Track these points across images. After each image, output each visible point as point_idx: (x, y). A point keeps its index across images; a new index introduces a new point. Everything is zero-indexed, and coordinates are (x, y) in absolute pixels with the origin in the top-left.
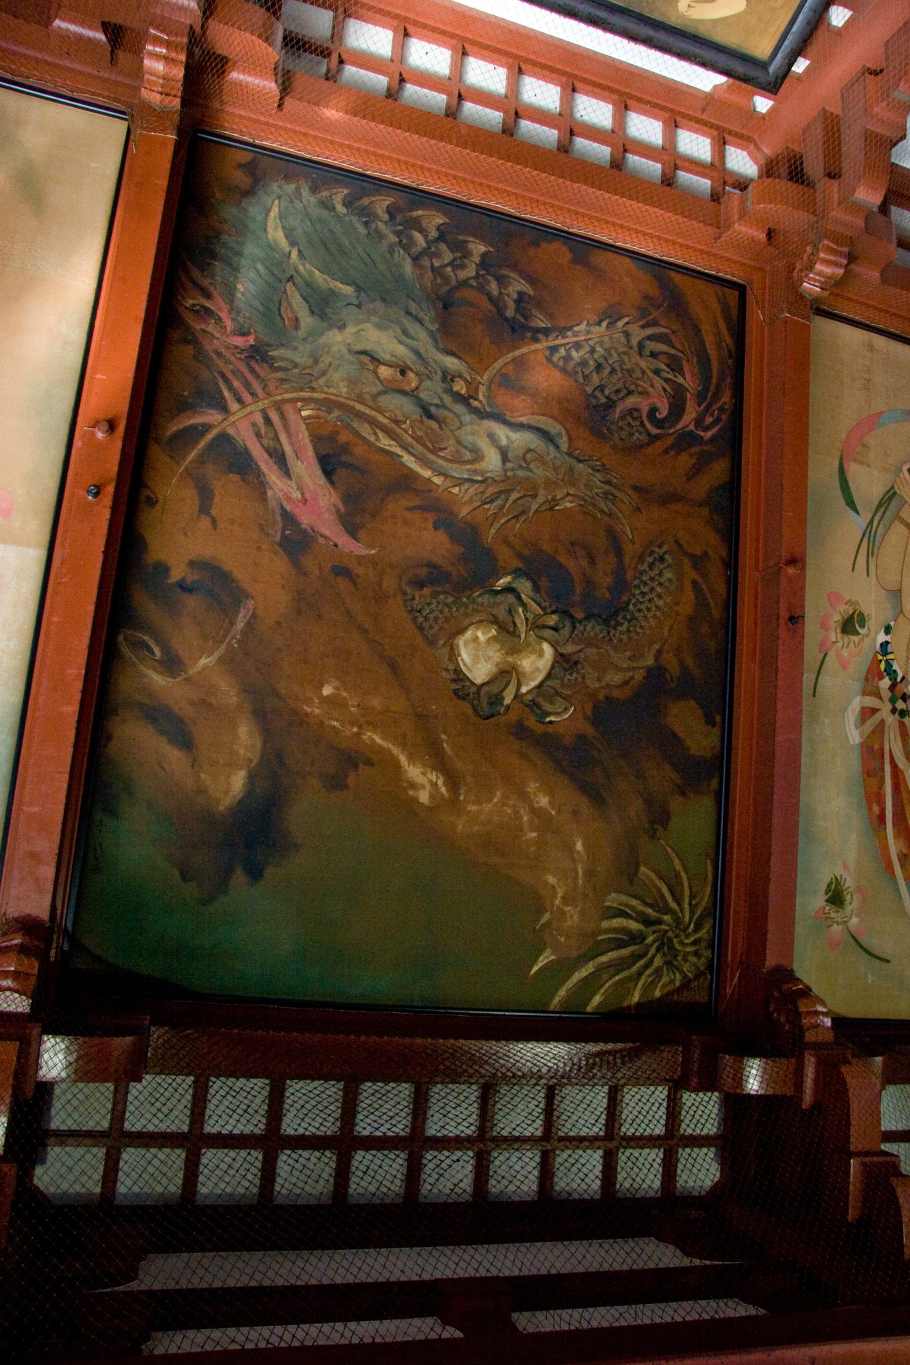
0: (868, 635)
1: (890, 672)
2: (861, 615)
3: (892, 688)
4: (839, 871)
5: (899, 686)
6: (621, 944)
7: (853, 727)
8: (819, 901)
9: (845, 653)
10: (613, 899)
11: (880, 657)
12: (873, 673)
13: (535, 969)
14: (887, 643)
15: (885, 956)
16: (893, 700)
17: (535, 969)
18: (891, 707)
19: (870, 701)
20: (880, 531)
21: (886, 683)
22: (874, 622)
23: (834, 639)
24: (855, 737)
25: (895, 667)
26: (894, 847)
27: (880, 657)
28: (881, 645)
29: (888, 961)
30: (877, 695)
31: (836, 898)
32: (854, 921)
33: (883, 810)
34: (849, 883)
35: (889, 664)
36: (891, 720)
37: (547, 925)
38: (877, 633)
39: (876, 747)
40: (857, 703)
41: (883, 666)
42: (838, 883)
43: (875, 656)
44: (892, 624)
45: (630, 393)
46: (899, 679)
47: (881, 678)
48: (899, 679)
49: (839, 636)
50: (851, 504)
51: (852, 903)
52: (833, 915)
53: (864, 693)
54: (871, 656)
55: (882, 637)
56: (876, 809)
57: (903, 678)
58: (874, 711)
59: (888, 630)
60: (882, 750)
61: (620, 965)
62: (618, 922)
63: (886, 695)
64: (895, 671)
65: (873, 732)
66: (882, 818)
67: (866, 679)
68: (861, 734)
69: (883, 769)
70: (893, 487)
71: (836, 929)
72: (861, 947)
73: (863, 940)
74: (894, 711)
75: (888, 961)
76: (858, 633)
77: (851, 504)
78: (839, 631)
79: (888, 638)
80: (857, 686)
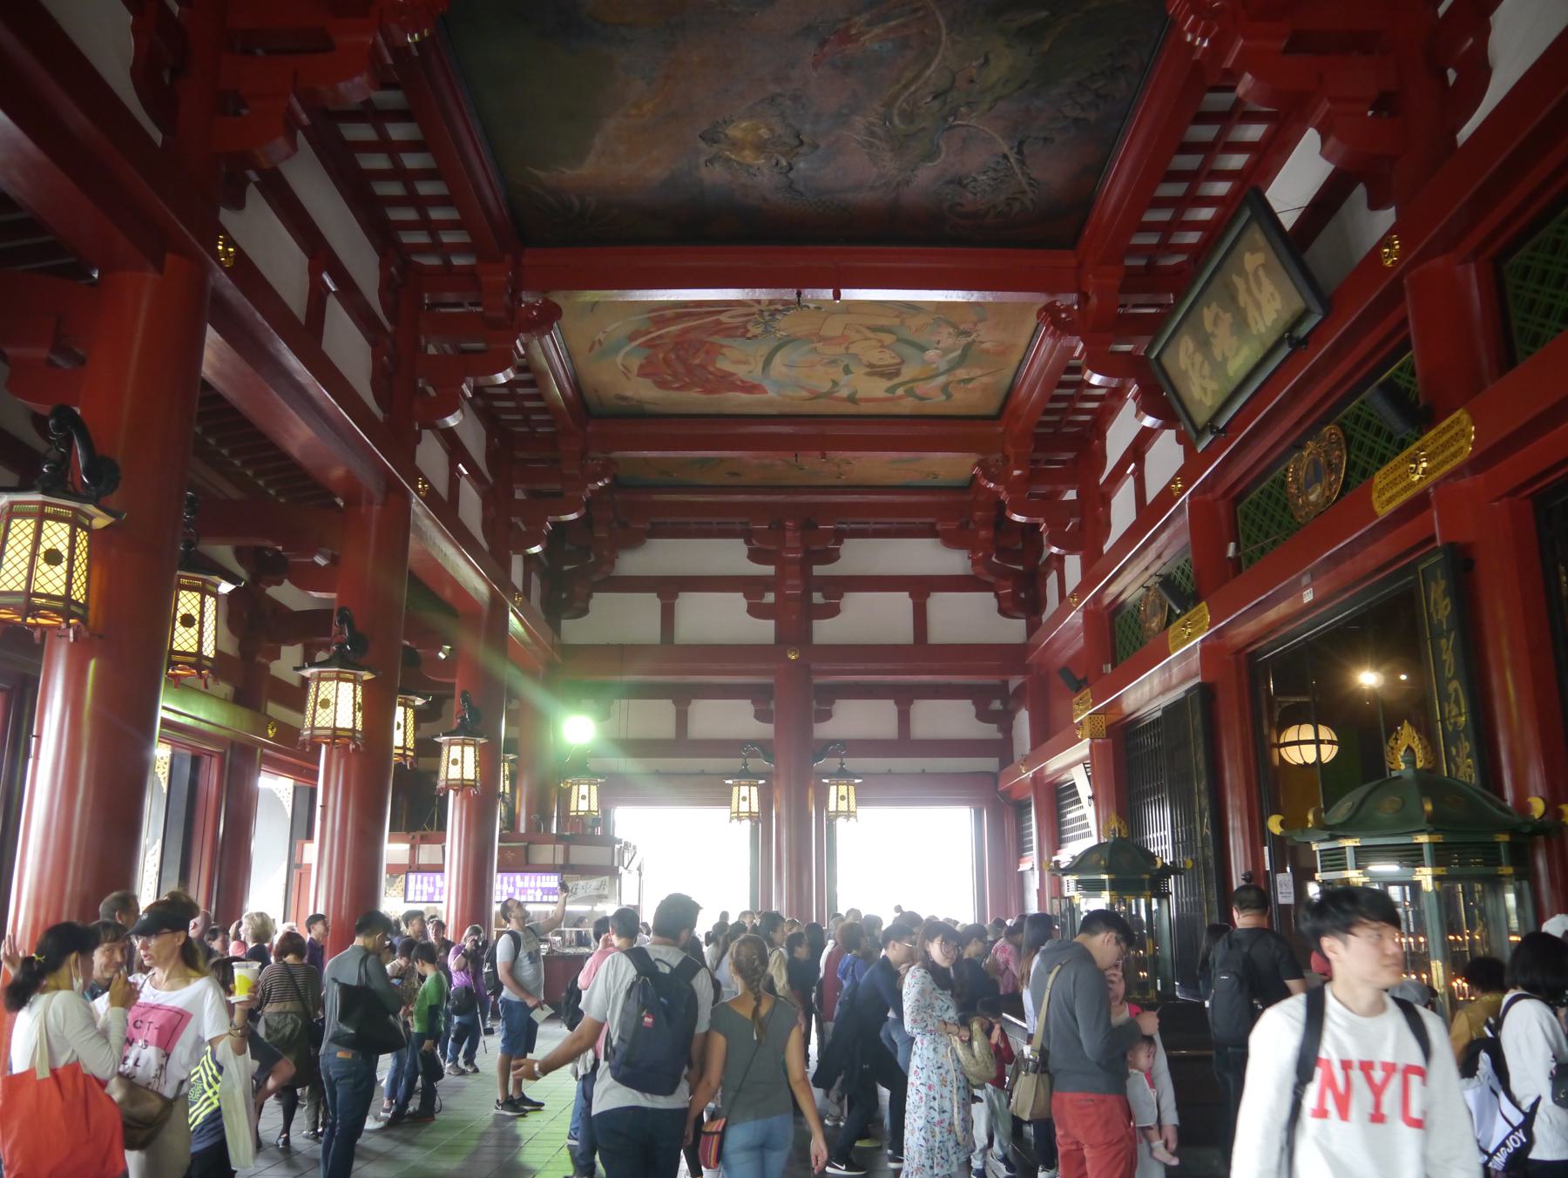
21: (780, 307)
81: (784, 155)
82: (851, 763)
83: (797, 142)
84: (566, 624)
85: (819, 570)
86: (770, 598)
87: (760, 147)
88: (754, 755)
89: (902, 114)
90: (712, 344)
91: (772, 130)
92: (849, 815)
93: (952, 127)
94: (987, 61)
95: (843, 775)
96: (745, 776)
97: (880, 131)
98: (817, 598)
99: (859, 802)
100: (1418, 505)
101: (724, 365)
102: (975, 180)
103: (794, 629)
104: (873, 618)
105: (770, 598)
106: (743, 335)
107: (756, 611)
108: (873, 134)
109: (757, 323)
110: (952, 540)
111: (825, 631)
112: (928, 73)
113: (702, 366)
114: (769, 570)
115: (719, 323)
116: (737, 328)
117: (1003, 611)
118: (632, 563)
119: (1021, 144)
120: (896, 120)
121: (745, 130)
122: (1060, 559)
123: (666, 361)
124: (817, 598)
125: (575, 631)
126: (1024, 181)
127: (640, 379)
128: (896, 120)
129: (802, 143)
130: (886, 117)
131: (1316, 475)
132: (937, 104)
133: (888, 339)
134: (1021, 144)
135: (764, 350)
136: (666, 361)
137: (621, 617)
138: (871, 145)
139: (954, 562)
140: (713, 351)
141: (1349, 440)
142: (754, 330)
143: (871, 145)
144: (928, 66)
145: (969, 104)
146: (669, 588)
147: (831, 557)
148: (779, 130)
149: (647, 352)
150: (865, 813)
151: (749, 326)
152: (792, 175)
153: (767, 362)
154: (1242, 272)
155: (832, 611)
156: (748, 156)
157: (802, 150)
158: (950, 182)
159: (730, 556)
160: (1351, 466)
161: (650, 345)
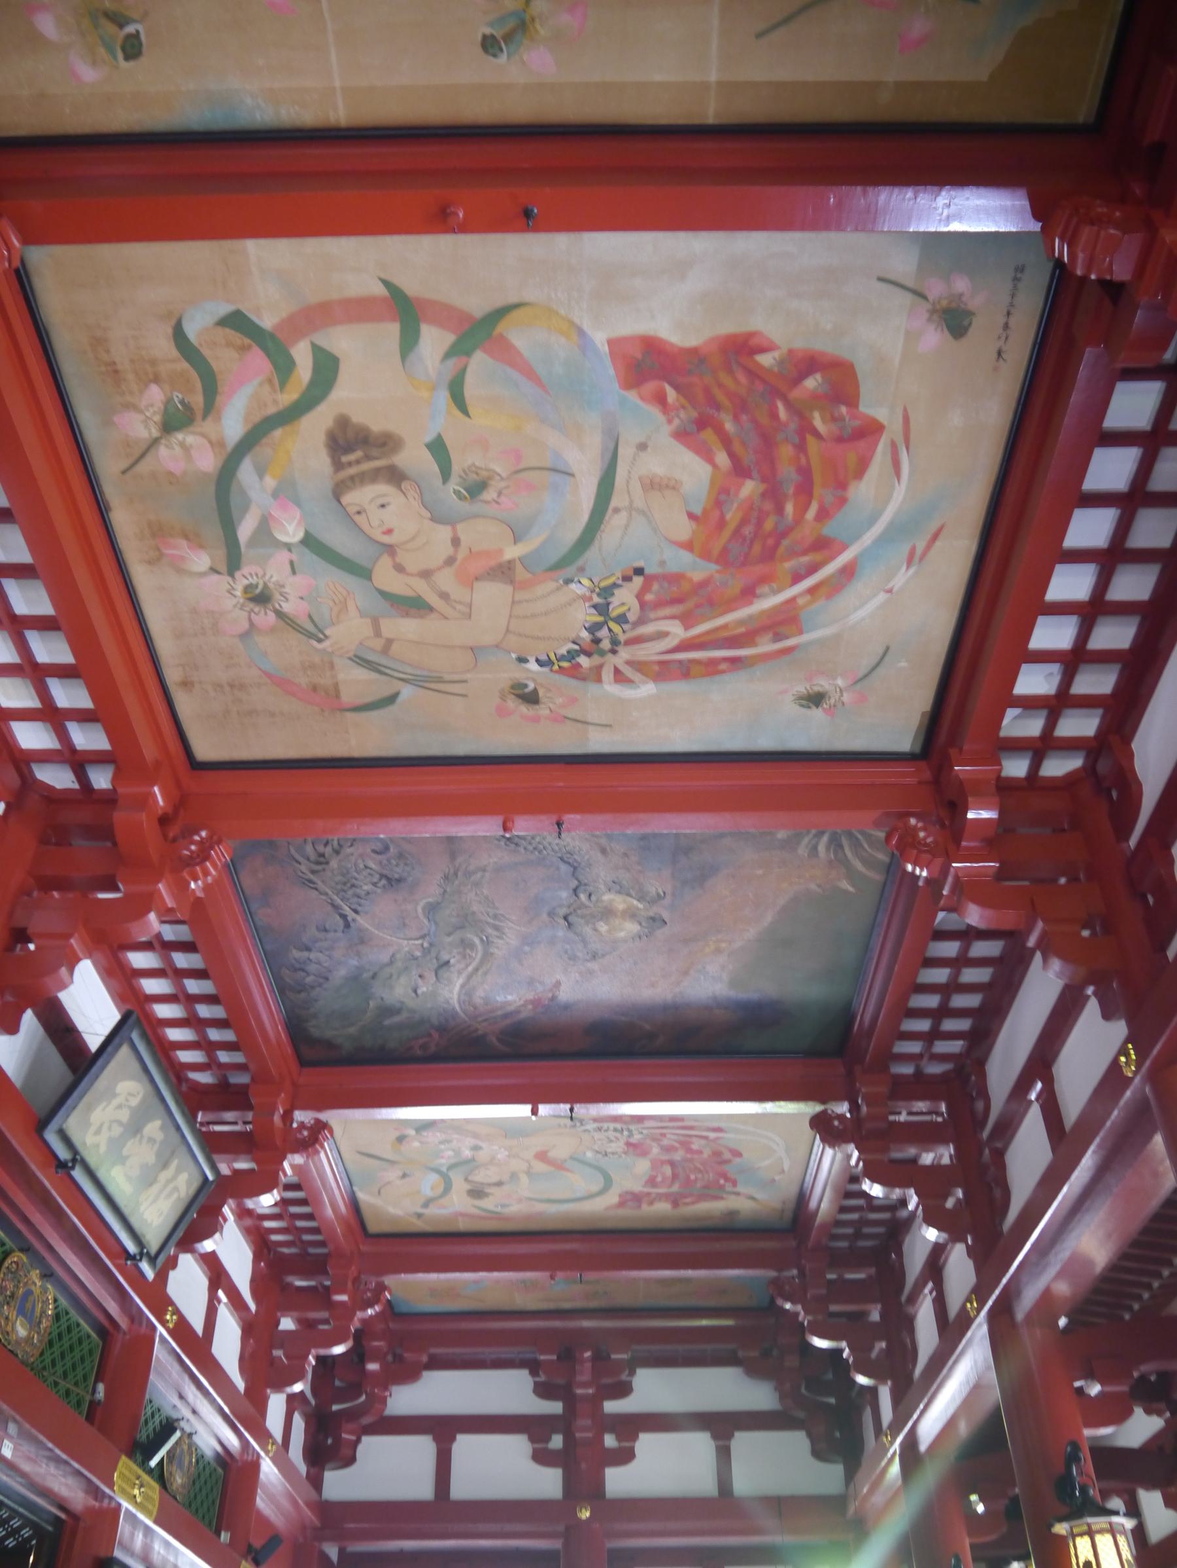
0: (534, 680)
1: (571, 656)
2: (513, 687)
3: (589, 654)
4: (789, 698)
5: (587, 648)
6: (841, 846)
7: (639, 691)
8: (817, 713)
9: (560, 701)
10: (802, 850)
11: (556, 667)
12: (574, 671)
13: (851, 889)
14: (537, 660)
15: (881, 651)
16: (602, 653)
17: (851, 889)
18: (610, 655)
19: (607, 675)
20: (409, 670)
21: (583, 660)
22: (516, 673)
23: (548, 712)
24: (648, 689)
25: (563, 651)
26: (766, 646)
27: (556, 667)
28: (541, 666)
29: (888, 648)
30: (599, 668)
31: (815, 699)
32: (840, 682)
33: (726, 659)
34: (802, 688)
35: (561, 658)
36: (624, 654)
37: (819, 886)
38: (528, 670)
39: (656, 668)
40: (610, 687)
41: (565, 664)
42: (801, 698)
43: (556, 672)
44: (514, 656)
45: (366, 867)
46: (577, 647)
47: (579, 665)
48: (577, 647)
49: (542, 706)
50: (392, 699)
51: (822, 684)
52: (832, 701)
53: (599, 680)
54: (557, 677)
55: (533, 666)
56: (723, 666)
57: (574, 642)
58: (617, 671)
59: (522, 660)
60: (662, 663)
61: (856, 845)
62: (822, 848)
63: (596, 660)
64: (568, 652)
65: (640, 671)
66: (734, 661)
67: (584, 679)
68: (645, 683)
69: (680, 662)
70: (350, 659)
71: (846, 697)
72: (866, 676)
73: (860, 675)
74: (614, 652)
75: (888, 648)
76: (535, 691)
77: (392, 699)
78: (537, 707)
79: (532, 660)
80: (592, 688)
81: (583, 906)
83: (570, 919)
87: (608, 913)
89: (472, 946)
90: (705, 555)
91: (596, 930)
93: (423, 937)
94: (415, 992)
97: (490, 931)
98: (610, 1441)
102: (375, 884)
106: (649, 580)
108: (497, 928)
109: (622, 619)
112: (460, 981)
113: (740, 471)
115: (687, 620)
116: (659, 604)
119: (347, 925)
120: (477, 941)
121: (622, 930)
124: (610, 1441)
126: (320, 885)
127: (881, 414)
128: (477, 941)
129: (565, 918)
130: (487, 943)
132: (445, 957)
134: (347, 925)
138: (495, 917)
142: (625, 599)
143: (495, 917)
144: (463, 986)
145: (416, 959)
148: (587, 930)
149: (830, 529)
151: (636, 605)
152: (575, 883)
156: (619, 902)
157: (563, 911)
158: (399, 881)
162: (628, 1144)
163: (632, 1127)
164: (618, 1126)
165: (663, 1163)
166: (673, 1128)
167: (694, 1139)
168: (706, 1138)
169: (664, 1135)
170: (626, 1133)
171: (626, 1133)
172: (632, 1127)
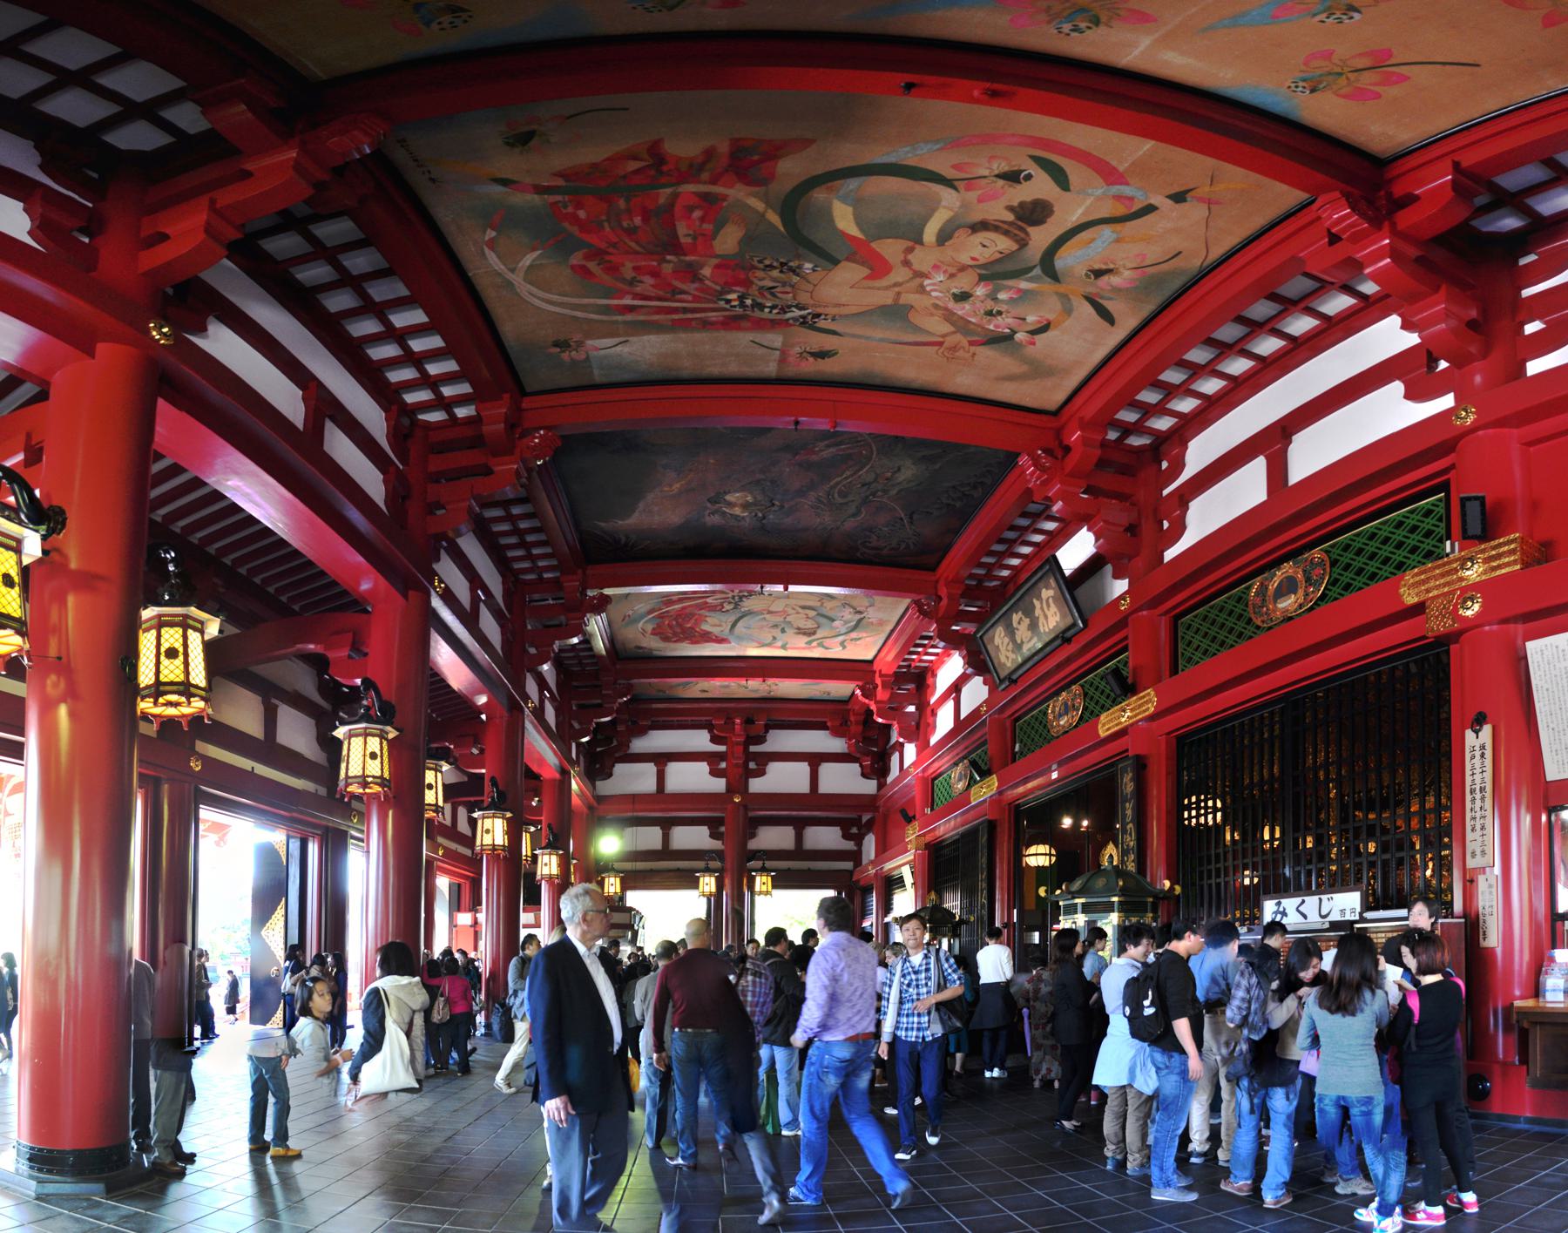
82: (768, 864)
84: (598, 783)
85: (753, 749)
86: (723, 765)
88: (713, 859)
92: (767, 893)
95: (763, 870)
96: (707, 870)
99: (774, 887)
100: (1122, 733)
101: (705, 627)
103: (737, 784)
104: (785, 778)
105: (723, 765)
107: (715, 773)
110: (837, 733)
111: (757, 785)
114: (722, 748)
117: (864, 775)
118: (640, 745)
122: (902, 745)
123: (670, 626)
125: (606, 787)
131: (1066, 709)
133: (812, 613)
135: (733, 618)
136: (670, 626)
137: (635, 779)
139: (837, 745)
140: (701, 619)
141: (1085, 695)
142: (727, 607)
146: (662, 759)
147: (761, 740)
150: (778, 893)
153: (734, 625)
154: (1039, 598)
155: (761, 772)
159: (700, 740)
160: (1085, 708)
161: (661, 616)
162: (747, 283)
163: (739, 310)
164: (757, 314)
165: (693, 249)
166: (685, 310)
167: (652, 292)
168: (636, 296)
169: (696, 299)
170: (749, 302)
171: (749, 302)
172: (739, 310)
